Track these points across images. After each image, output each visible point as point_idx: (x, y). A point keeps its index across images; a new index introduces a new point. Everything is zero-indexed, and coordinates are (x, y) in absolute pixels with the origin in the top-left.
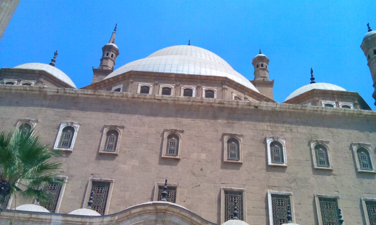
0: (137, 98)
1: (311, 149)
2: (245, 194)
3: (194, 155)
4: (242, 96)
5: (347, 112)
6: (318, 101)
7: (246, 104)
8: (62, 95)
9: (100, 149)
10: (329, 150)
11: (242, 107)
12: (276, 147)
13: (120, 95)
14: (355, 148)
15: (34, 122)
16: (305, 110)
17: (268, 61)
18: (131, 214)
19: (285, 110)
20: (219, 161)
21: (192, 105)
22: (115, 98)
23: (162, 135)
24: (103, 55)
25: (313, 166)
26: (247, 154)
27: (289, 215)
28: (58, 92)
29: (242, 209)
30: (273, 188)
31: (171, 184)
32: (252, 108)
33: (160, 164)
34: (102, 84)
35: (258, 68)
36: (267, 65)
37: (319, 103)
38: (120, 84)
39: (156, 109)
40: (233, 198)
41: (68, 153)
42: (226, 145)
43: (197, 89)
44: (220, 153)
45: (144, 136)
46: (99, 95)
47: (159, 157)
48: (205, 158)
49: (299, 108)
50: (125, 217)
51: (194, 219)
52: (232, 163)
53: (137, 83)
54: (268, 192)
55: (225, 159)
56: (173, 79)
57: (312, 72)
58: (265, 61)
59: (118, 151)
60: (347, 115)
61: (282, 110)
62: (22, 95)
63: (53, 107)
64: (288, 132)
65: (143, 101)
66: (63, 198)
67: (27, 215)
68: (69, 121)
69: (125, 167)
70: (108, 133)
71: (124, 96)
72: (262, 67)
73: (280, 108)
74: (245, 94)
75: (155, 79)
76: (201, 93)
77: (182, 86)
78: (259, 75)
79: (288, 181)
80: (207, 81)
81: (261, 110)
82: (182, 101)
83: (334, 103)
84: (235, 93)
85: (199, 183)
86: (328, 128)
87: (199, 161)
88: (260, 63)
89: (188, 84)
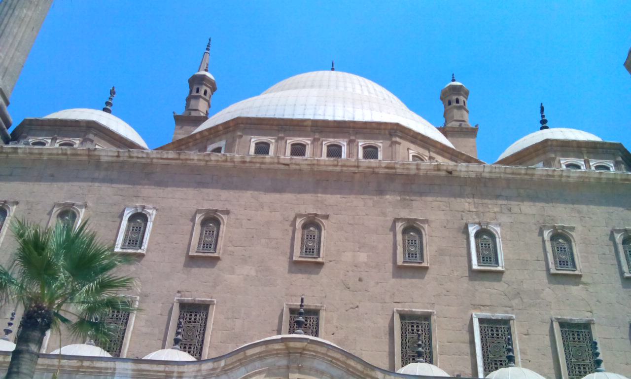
0: (250, 162)
1: (544, 241)
3: (347, 257)
4: (426, 153)
5: (603, 176)
6: (554, 159)
7: (432, 167)
8: (125, 161)
9: (191, 250)
10: (575, 241)
11: (425, 172)
12: (485, 239)
13: (221, 158)
14: (619, 238)
15: (81, 206)
16: (533, 175)
17: (466, 94)
18: (246, 356)
20: (390, 265)
21: (342, 171)
22: (213, 163)
23: (293, 224)
24: (191, 92)
25: (548, 269)
26: (436, 251)
27: (511, 354)
28: (118, 156)
29: (430, 345)
30: (482, 307)
31: (310, 306)
32: (443, 173)
34: (191, 140)
35: (450, 106)
36: (465, 100)
37: (556, 162)
38: (220, 140)
39: (281, 180)
40: (415, 326)
42: (399, 237)
43: (349, 144)
44: (391, 251)
45: (263, 226)
46: (187, 160)
47: (288, 260)
48: (366, 260)
49: (523, 172)
50: (236, 362)
51: (352, 363)
52: (412, 267)
53: (249, 137)
54: (474, 315)
55: (400, 262)
56: (309, 129)
57: (542, 109)
58: (462, 93)
59: (221, 252)
60: (604, 181)
61: (493, 176)
62: (59, 163)
63: (111, 181)
64: (503, 213)
65: (260, 167)
66: (133, 332)
67: (74, 363)
68: (139, 204)
70: (204, 223)
71: (229, 160)
72: (458, 105)
73: (490, 172)
74: (429, 151)
75: (279, 131)
76: (355, 150)
77: (325, 140)
78: (453, 117)
79: (506, 295)
80: (365, 130)
81: (459, 177)
82: (325, 165)
83: (581, 162)
84: (414, 150)
85: (358, 304)
86: (573, 204)
87: (356, 266)
88: (453, 97)
89: (334, 137)
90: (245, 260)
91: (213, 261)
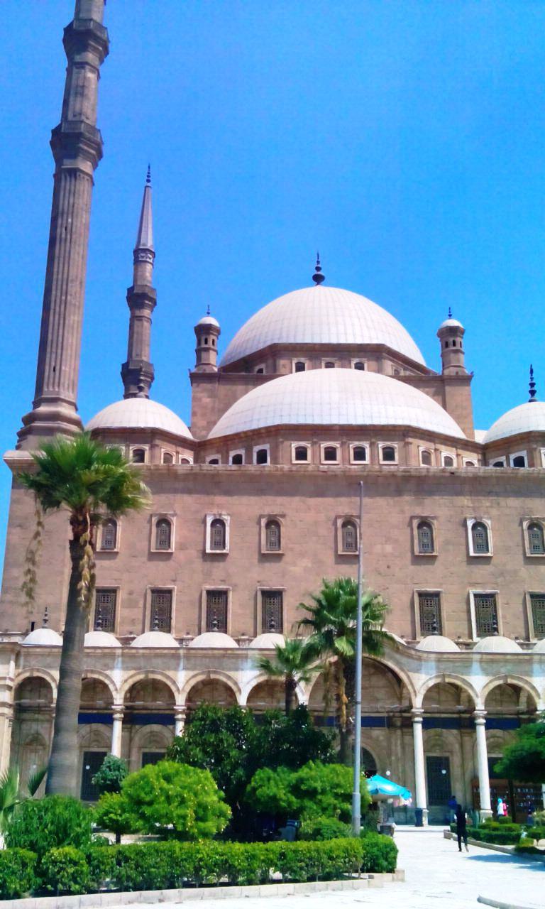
1: (523, 530)
2: (443, 596)
3: (378, 549)
4: (430, 446)
6: (535, 449)
16: (517, 473)
17: (463, 332)
19: (490, 474)
20: (409, 554)
22: (267, 472)
23: (335, 523)
24: (199, 343)
27: (495, 626)
28: (192, 470)
29: (440, 615)
32: (447, 474)
33: (337, 563)
37: (538, 451)
38: (264, 443)
39: (322, 485)
41: (224, 556)
42: (416, 532)
43: (371, 446)
52: (425, 557)
53: (287, 443)
55: (417, 553)
57: (532, 372)
61: (486, 475)
63: (189, 492)
67: (221, 652)
69: (297, 570)
70: (268, 525)
72: (454, 348)
73: (484, 473)
75: (312, 435)
76: (376, 452)
78: (450, 362)
81: (459, 477)
84: (423, 446)
85: (387, 586)
88: (449, 337)
90: (302, 555)
91: (279, 557)
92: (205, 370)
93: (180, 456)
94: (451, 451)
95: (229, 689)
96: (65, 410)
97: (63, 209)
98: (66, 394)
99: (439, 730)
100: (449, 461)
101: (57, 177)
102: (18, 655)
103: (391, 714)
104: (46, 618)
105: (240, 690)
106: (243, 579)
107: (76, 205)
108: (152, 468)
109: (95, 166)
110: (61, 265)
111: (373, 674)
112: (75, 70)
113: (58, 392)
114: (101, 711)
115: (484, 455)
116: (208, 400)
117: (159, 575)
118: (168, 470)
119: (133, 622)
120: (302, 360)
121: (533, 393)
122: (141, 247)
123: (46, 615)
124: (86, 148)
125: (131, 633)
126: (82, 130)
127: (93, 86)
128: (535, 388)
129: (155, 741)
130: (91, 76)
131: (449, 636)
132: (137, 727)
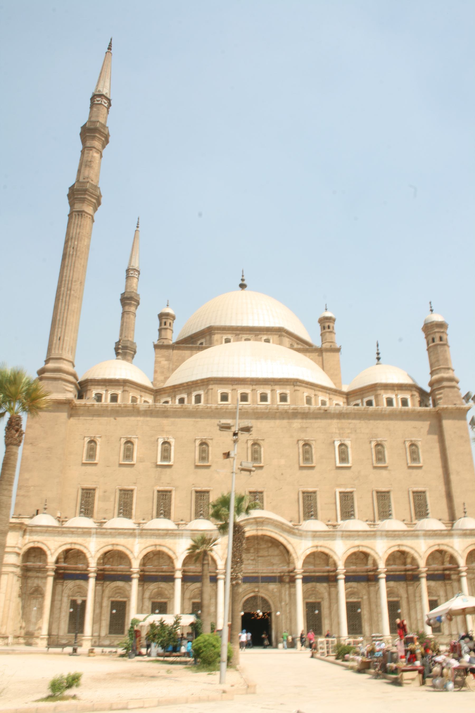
0: (220, 409)
2: (318, 493)
16: (368, 411)
17: (334, 320)
21: (269, 412)
24: (161, 324)
28: (149, 407)
32: (322, 411)
38: (200, 390)
57: (378, 346)
61: (348, 412)
72: (329, 330)
73: (346, 410)
78: (326, 339)
81: (330, 413)
84: (306, 393)
88: (326, 324)
89: (263, 388)
92: (163, 343)
93: (143, 398)
94: (326, 396)
95: (170, 558)
96: (65, 366)
97: (72, 236)
98: (66, 355)
99: (314, 584)
100: (324, 403)
101: (70, 216)
102: (25, 531)
103: (282, 574)
104: (46, 507)
105: (177, 558)
106: (183, 482)
107: (81, 234)
108: (122, 406)
109: (95, 210)
110: (69, 271)
111: (271, 547)
112: (86, 152)
113: (61, 354)
114: (83, 572)
115: (347, 399)
116: (166, 363)
117: (125, 478)
118: (133, 407)
119: (106, 511)
120: (229, 336)
121: (378, 359)
122: (131, 268)
123: (46, 505)
124: (89, 198)
125: (105, 519)
126: (88, 187)
127: (97, 162)
128: (380, 356)
129: (120, 593)
130: (96, 155)
131: (322, 520)
132: (108, 583)
